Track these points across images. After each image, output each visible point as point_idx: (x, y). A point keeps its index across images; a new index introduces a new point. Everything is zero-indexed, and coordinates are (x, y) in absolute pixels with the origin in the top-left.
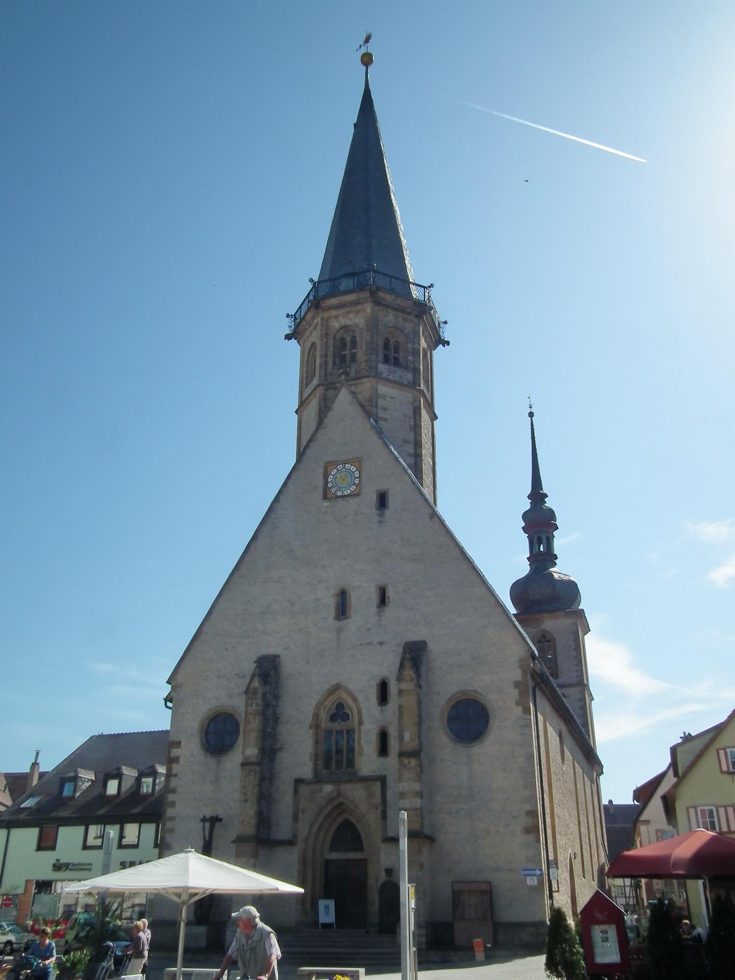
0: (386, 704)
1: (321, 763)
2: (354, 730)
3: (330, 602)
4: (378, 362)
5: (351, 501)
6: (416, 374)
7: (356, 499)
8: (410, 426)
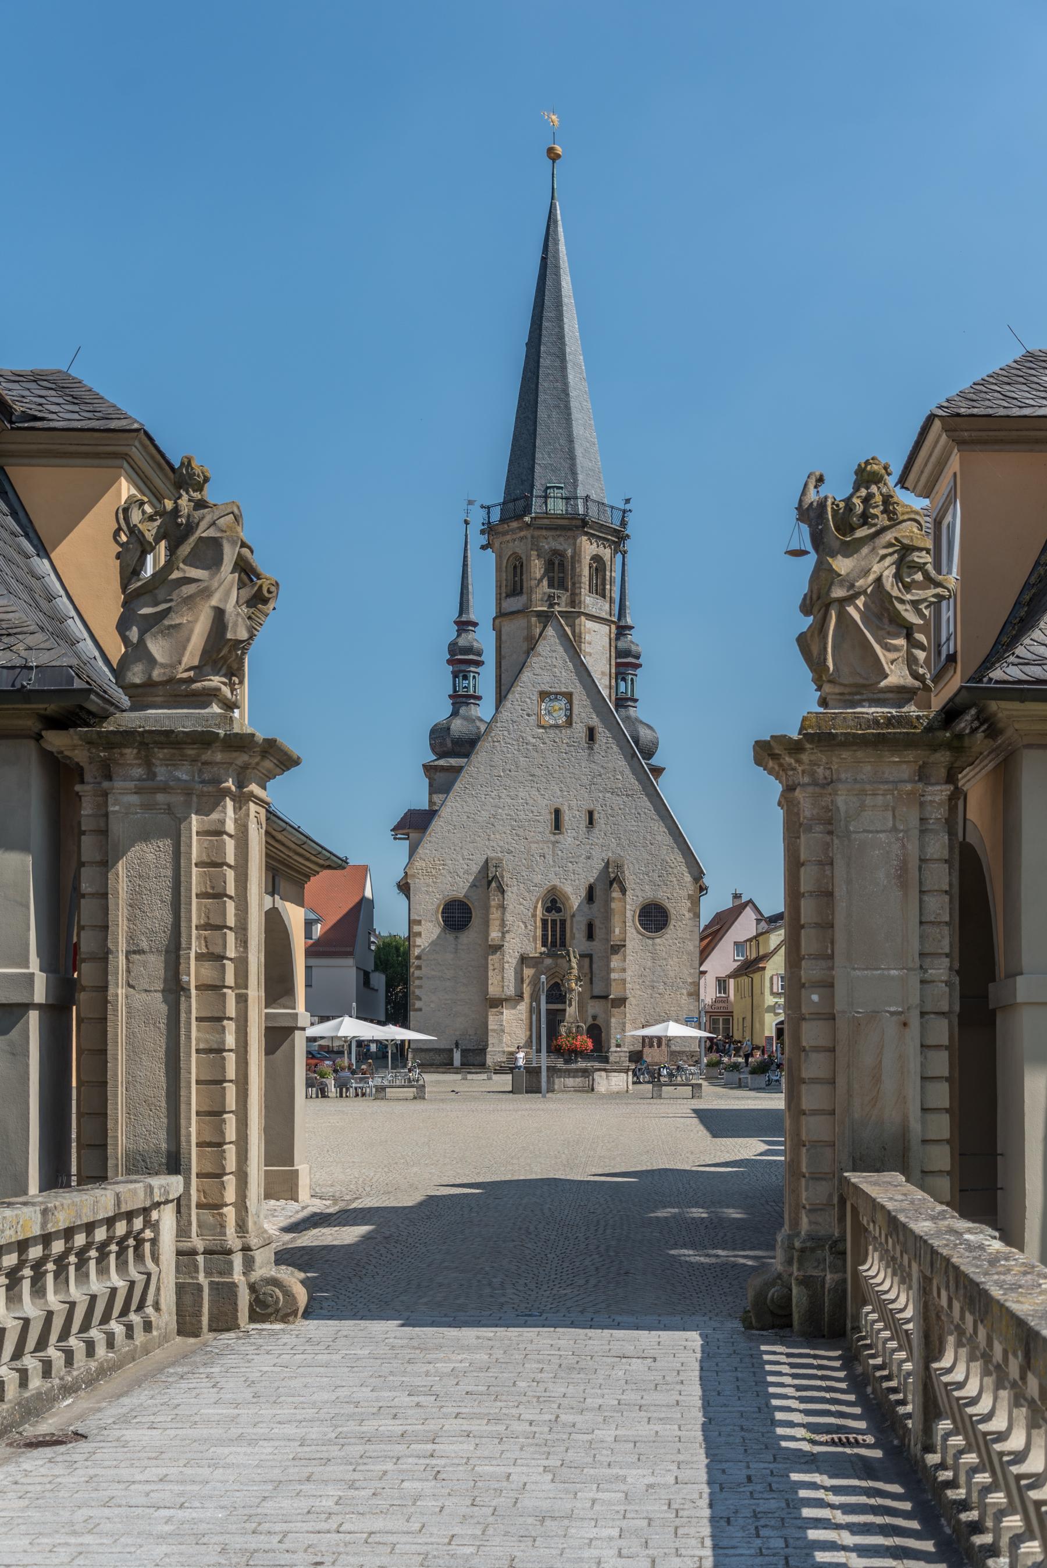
1: (539, 943)
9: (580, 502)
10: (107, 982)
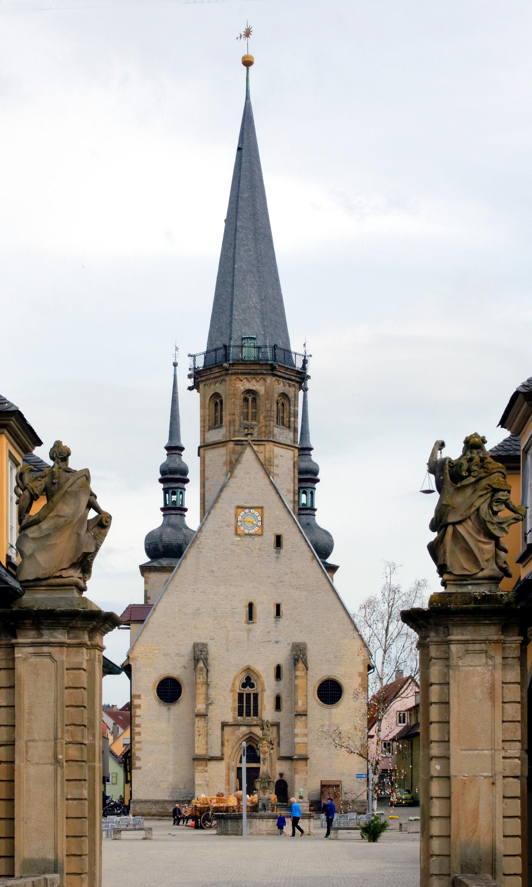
1: (237, 713)
3: (245, 611)
4: (274, 426)
5: (256, 539)
6: (296, 434)
8: (291, 477)
9: (268, 350)
10: (14, 758)
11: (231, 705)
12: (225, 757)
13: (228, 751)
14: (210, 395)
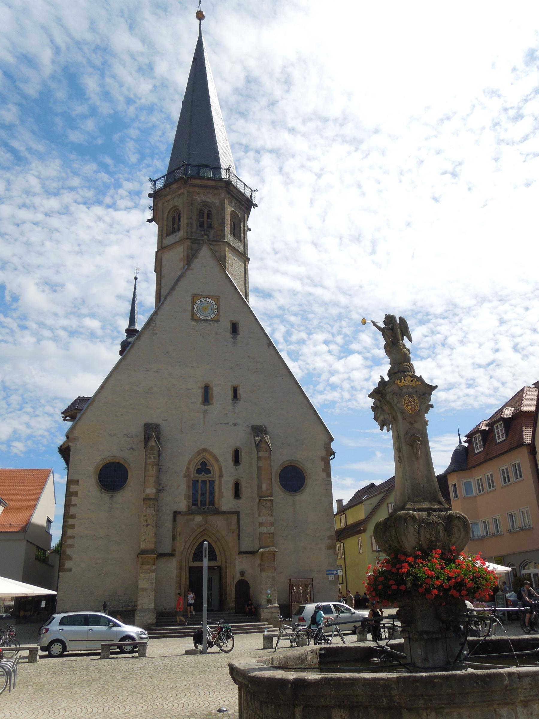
0: (239, 465)
2: (214, 481)
5: (213, 324)
7: (216, 324)
11: (184, 492)
12: (177, 553)
13: (180, 545)
14: (168, 210)
